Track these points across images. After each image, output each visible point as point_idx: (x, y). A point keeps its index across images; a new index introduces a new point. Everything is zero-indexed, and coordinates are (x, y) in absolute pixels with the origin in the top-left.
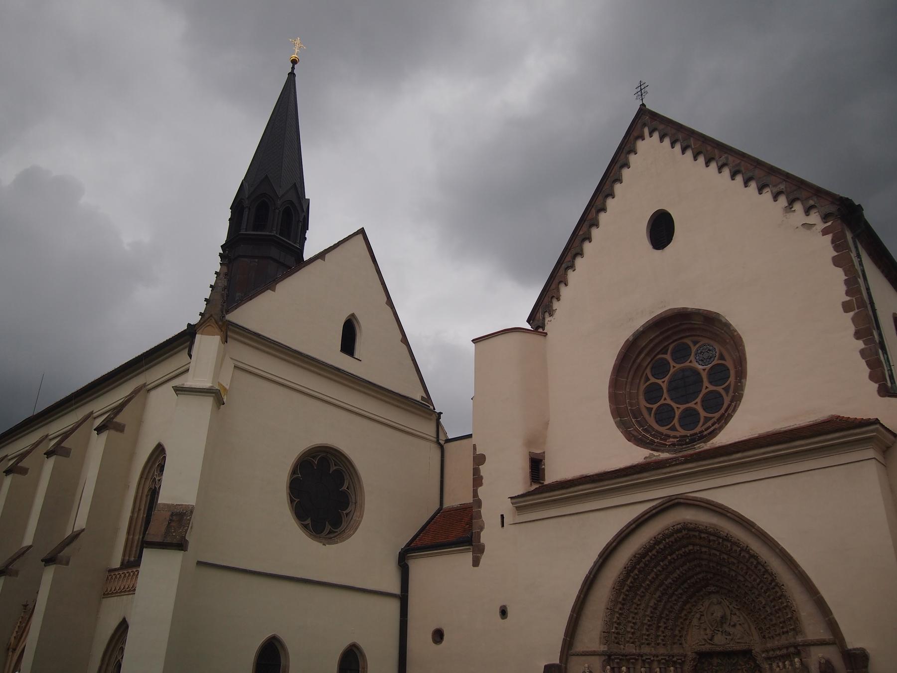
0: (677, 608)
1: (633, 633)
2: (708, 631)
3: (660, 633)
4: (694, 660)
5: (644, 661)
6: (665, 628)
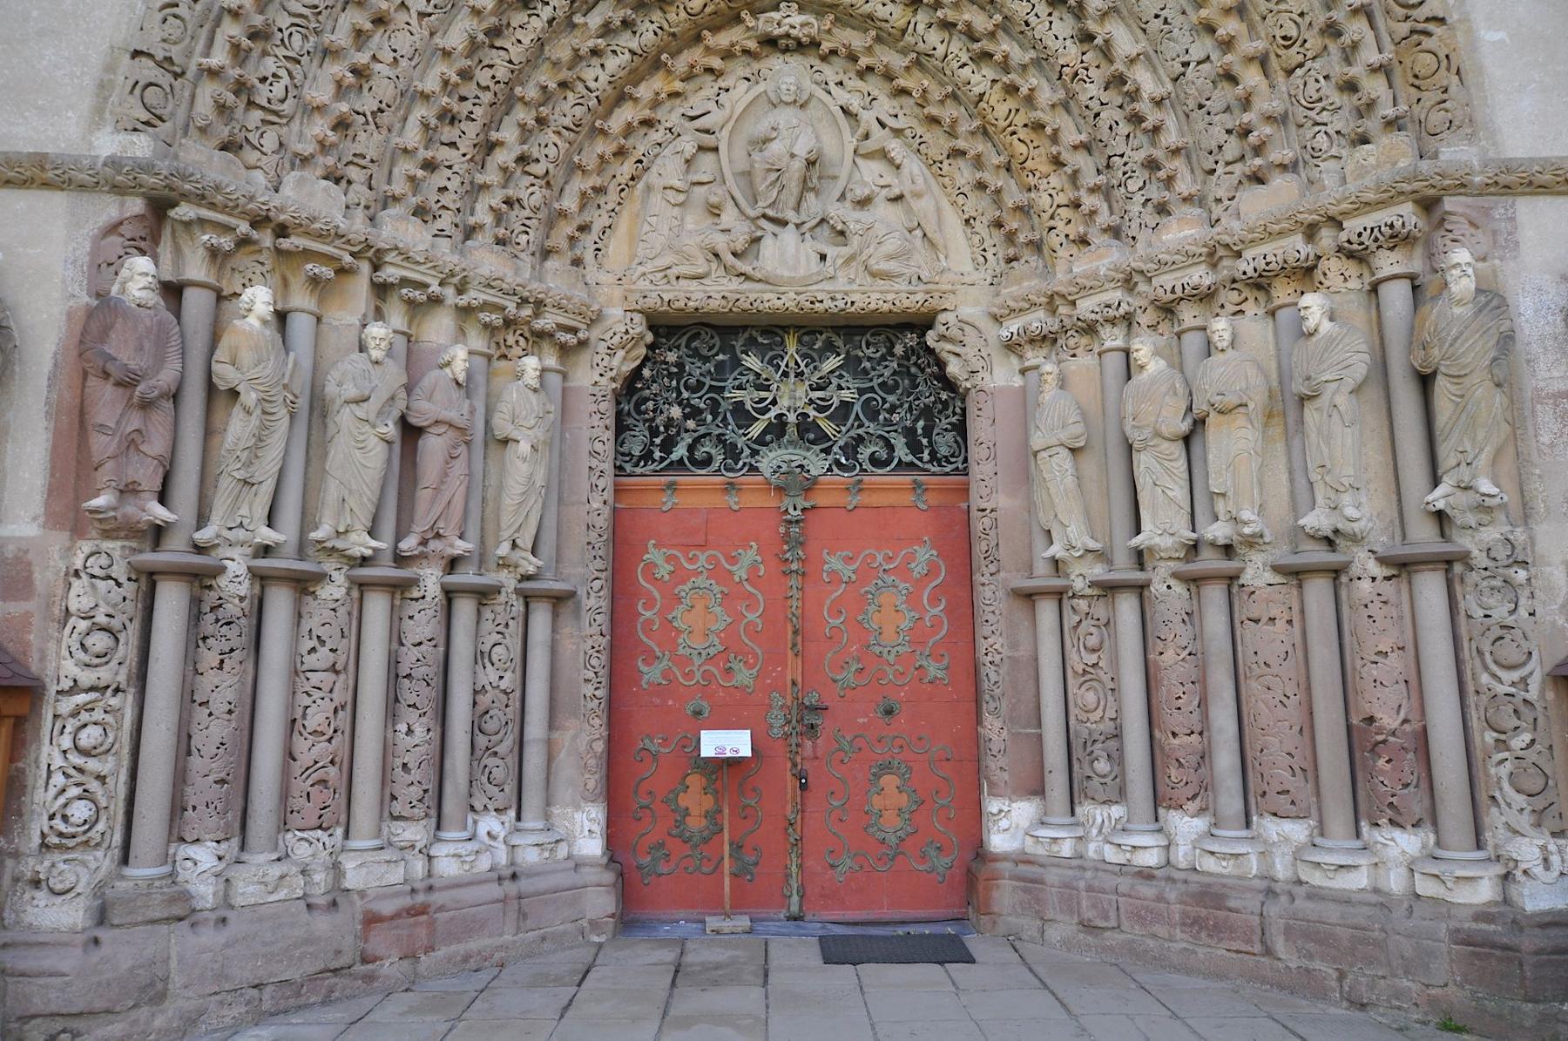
0: (597, 76)
1: (341, 125)
2: (729, 217)
3: (491, 176)
4: (630, 342)
5: (381, 290)
6: (522, 159)
